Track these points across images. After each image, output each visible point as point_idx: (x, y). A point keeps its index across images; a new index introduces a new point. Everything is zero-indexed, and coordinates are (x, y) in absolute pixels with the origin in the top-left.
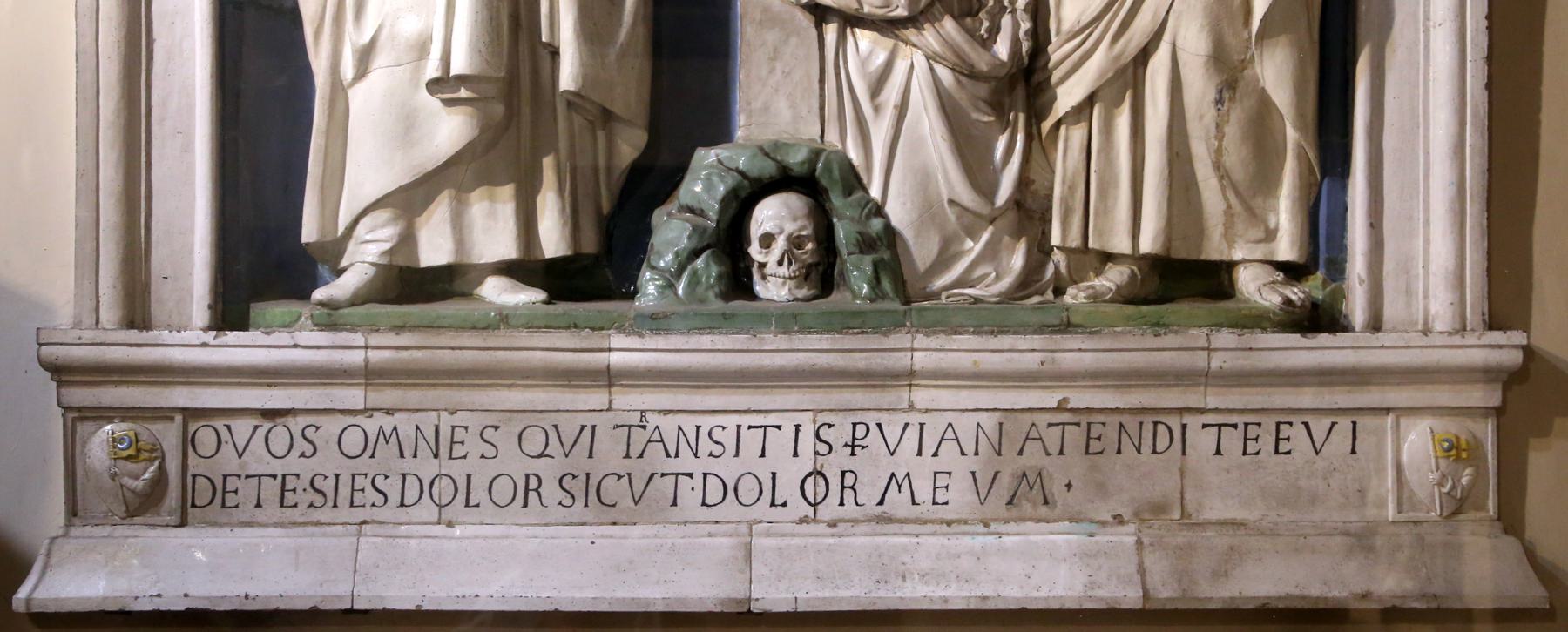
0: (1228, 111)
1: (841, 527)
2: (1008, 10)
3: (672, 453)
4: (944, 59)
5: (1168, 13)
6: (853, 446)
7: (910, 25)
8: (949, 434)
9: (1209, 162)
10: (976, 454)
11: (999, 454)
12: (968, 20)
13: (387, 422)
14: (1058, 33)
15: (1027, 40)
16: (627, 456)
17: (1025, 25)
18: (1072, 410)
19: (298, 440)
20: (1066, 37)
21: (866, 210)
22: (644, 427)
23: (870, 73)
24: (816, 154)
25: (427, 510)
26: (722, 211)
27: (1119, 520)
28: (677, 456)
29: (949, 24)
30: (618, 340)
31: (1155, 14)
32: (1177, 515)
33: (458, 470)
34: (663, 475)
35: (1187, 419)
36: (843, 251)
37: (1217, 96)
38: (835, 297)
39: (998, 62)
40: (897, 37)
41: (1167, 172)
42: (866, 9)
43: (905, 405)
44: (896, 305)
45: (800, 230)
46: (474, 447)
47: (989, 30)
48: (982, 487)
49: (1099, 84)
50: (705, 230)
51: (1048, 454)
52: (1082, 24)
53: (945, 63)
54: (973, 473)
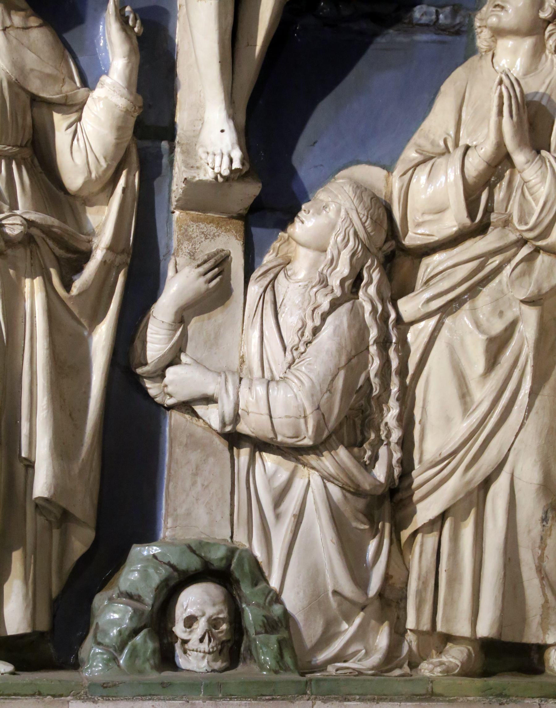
0: (551, 527)
2: (385, 443)
4: (337, 480)
5: (509, 450)
7: (310, 452)
9: (534, 567)
12: (356, 450)
14: (420, 462)
15: (398, 467)
17: (397, 455)
20: (429, 465)
21: (269, 598)
23: (274, 489)
24: (232, 551)
26: (155, 598)
29: (342, 452)
31: (500, 451)
36: (252, 631)
37: (544, 516)
38: (241, 668)
39: (378, 483)
40: (298, 460)
41: (503, 573)
42: (280, 439)
44: (296, 677)
45: (218, 614)
47: (370, 458)
49: (452, 503)
50: (143, 613)
52: (443, 456)
53: (337, 482)
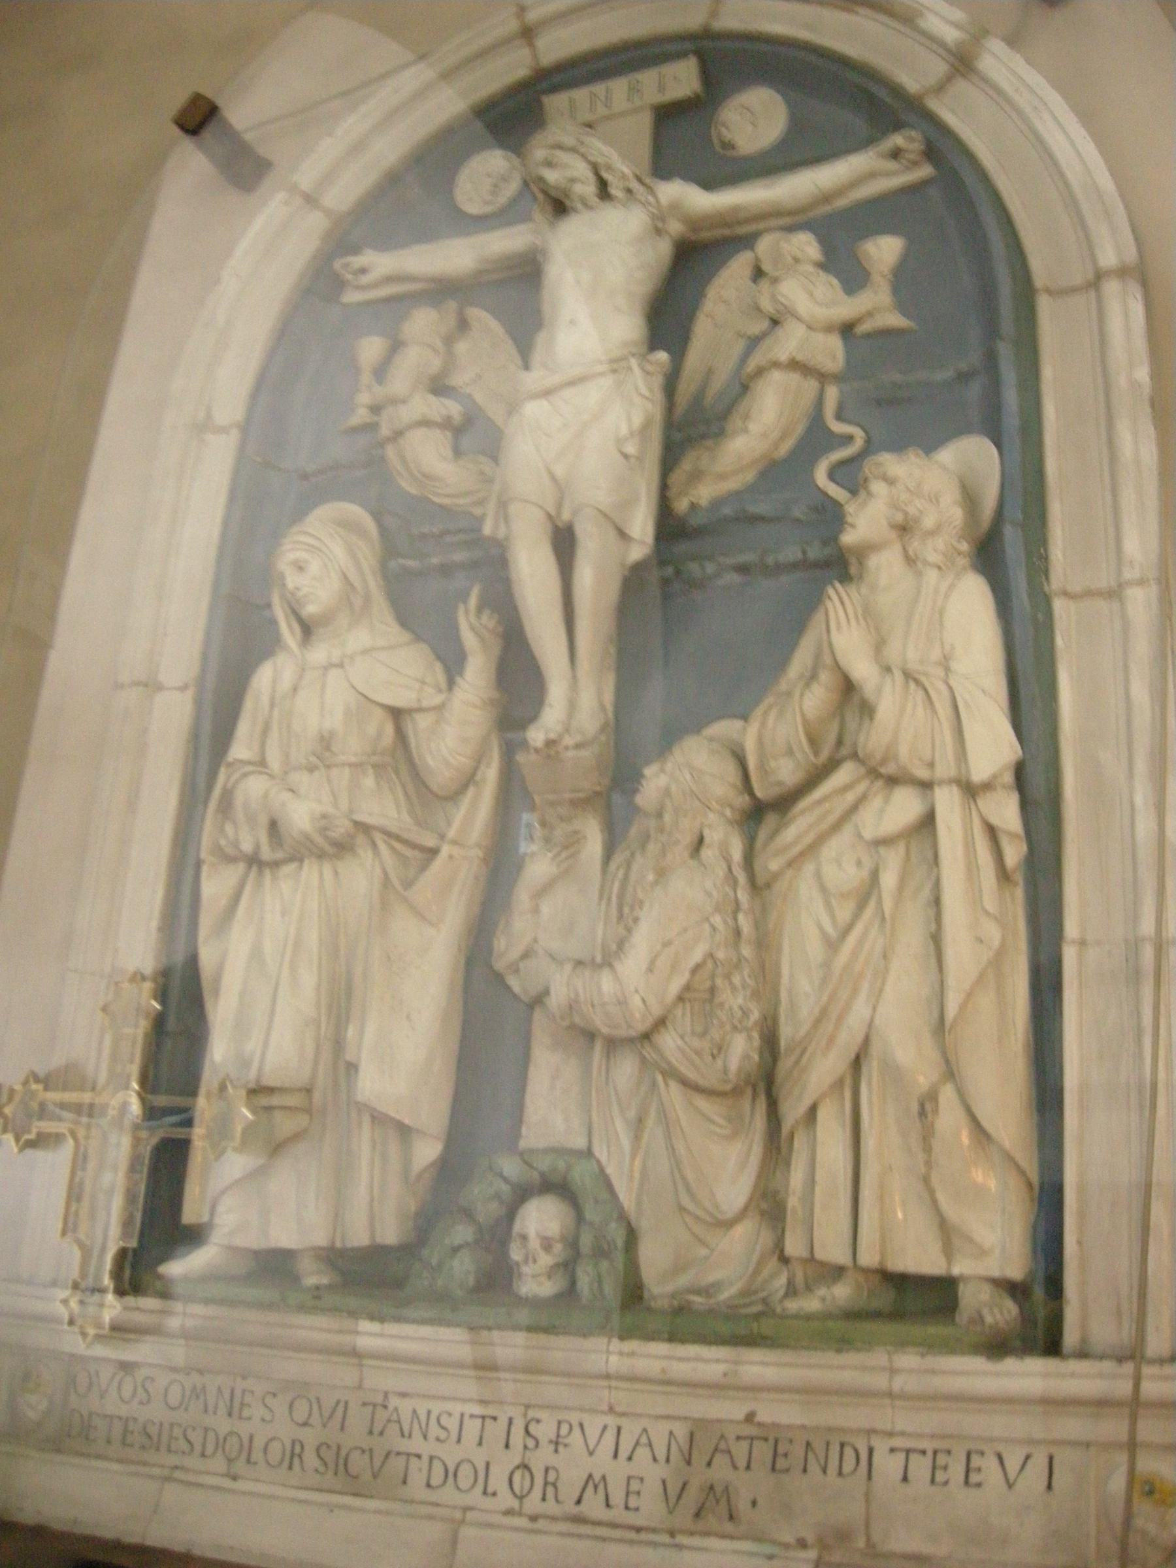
1: (541, 1524)
3: (406, 1434)
6: (557, 1443)
8: (644, 1440)
10: (668, 1460)
11: (689, 1463)
16: (371, 1433)
18: (760, 1424)
19: (140, 1390)
22: (385, 1407)
25: (218, 1464)
27: (802, 1544)
28: (410, 1436)
30: (365, 1325)
32: (861, 1543)
33: (244, 1429)
34: (398, 1454)
43: (605, 1408)
46: (257, 1411)
48: (673, 1497)
51: (735, 1467)
54: (664, 1482)
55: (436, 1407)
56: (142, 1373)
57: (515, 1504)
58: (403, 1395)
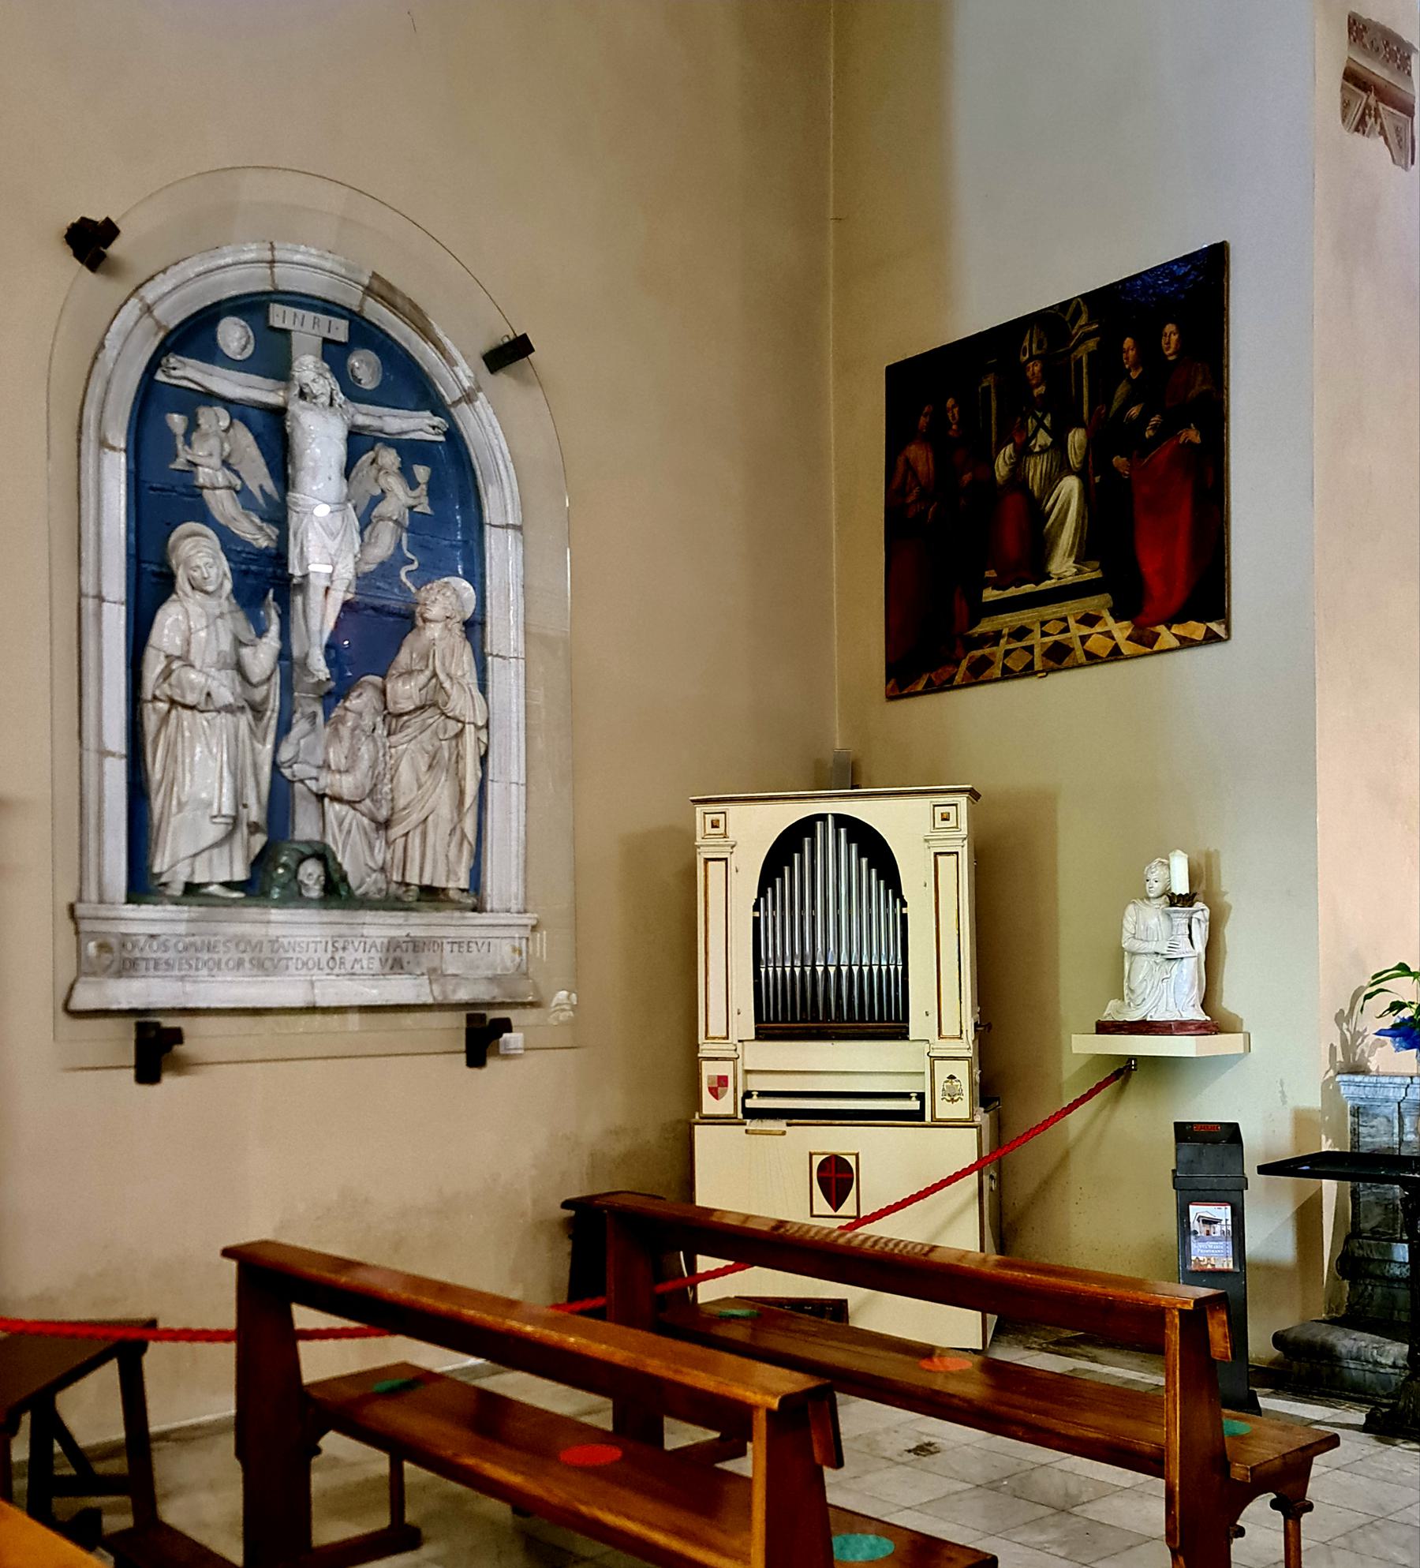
13: (192, 939)
25: (204, 972)
27: (423, 974)
30: (273, 911)
35: (445, 941)
46: (221, 948)
48: (383, 962)
55: (298, 939)
56: (163, 938)
57: (329, 971)
58: (284, 936)
